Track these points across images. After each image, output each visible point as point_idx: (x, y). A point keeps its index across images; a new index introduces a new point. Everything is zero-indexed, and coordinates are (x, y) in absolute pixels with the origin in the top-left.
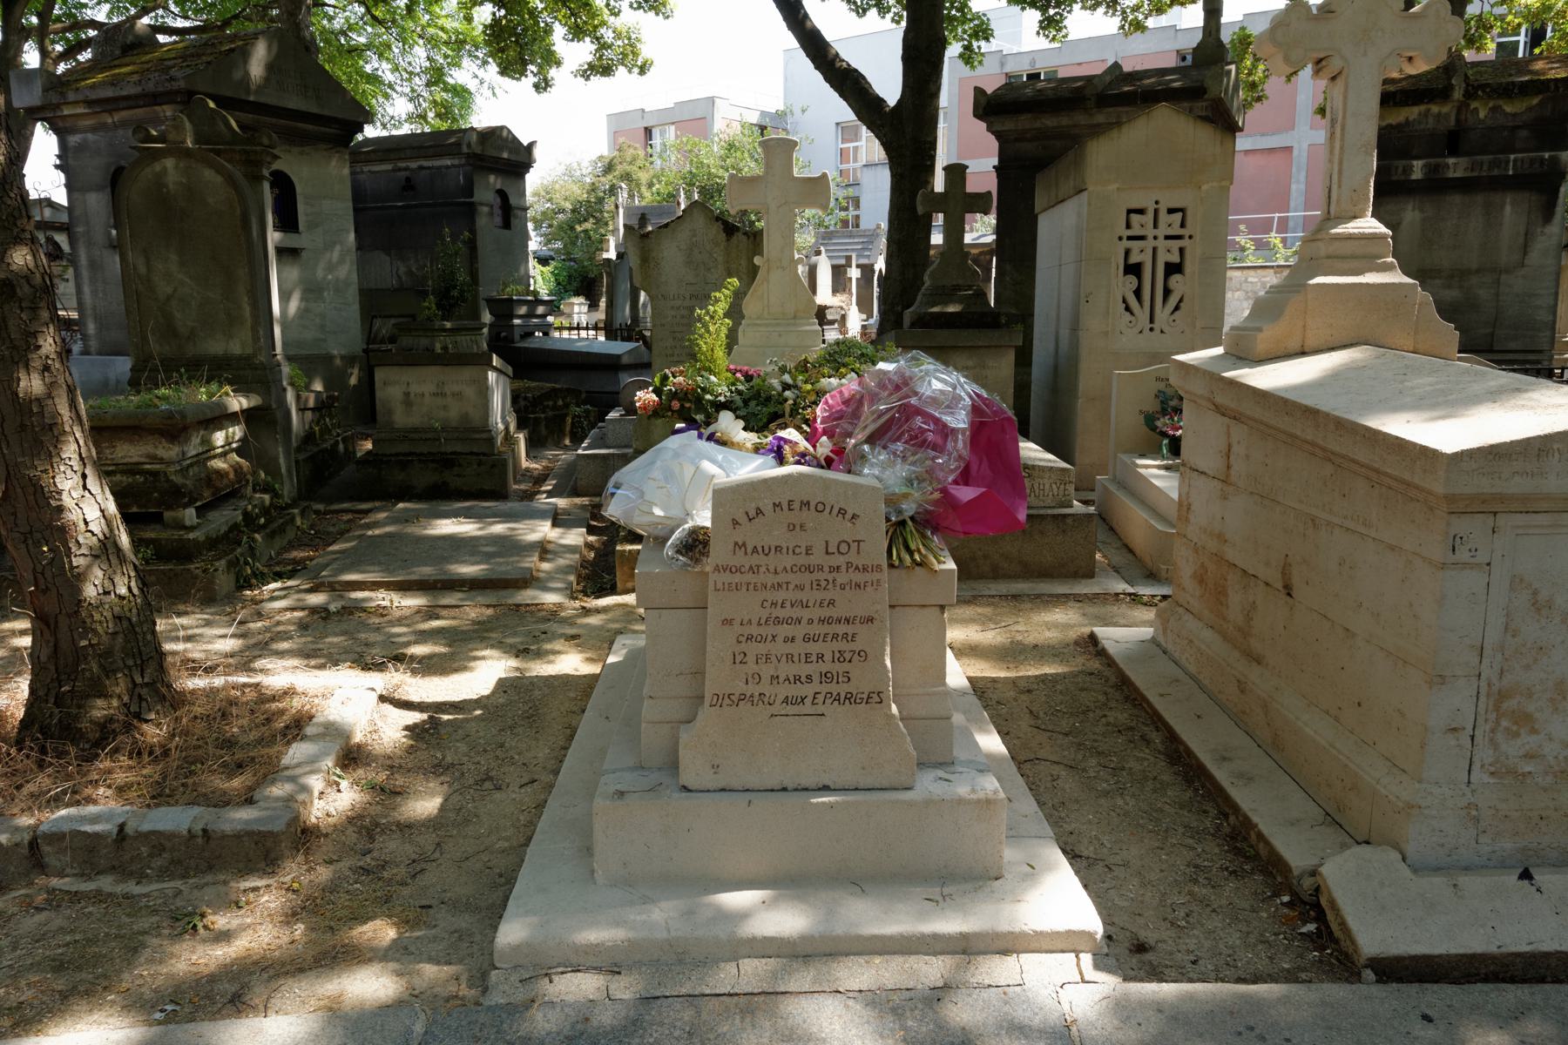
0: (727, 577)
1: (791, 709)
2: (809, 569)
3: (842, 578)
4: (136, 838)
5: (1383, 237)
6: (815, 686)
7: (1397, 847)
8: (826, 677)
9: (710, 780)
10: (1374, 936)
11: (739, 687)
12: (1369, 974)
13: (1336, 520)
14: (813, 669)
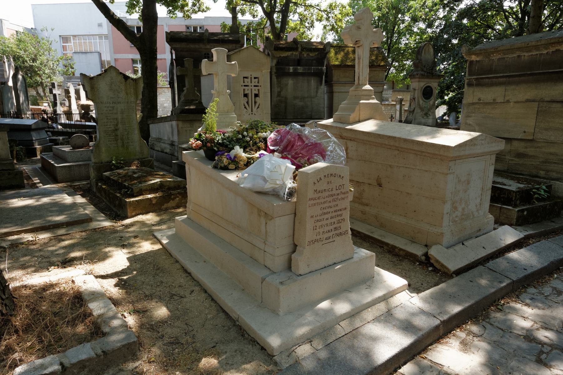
0: (312, 202)
1: (327, 241)
2: (332, 195)
3: (339, 197)
4: (71, 367)
5: (370, 90)
6: (333, 232)
7: (439, 244)
8: (336, 229)
9: (307, 270)
10: (453, 266)
11: (315, 237)
12: (455, 275)
13: (401, 165)
14: (332, 227)
